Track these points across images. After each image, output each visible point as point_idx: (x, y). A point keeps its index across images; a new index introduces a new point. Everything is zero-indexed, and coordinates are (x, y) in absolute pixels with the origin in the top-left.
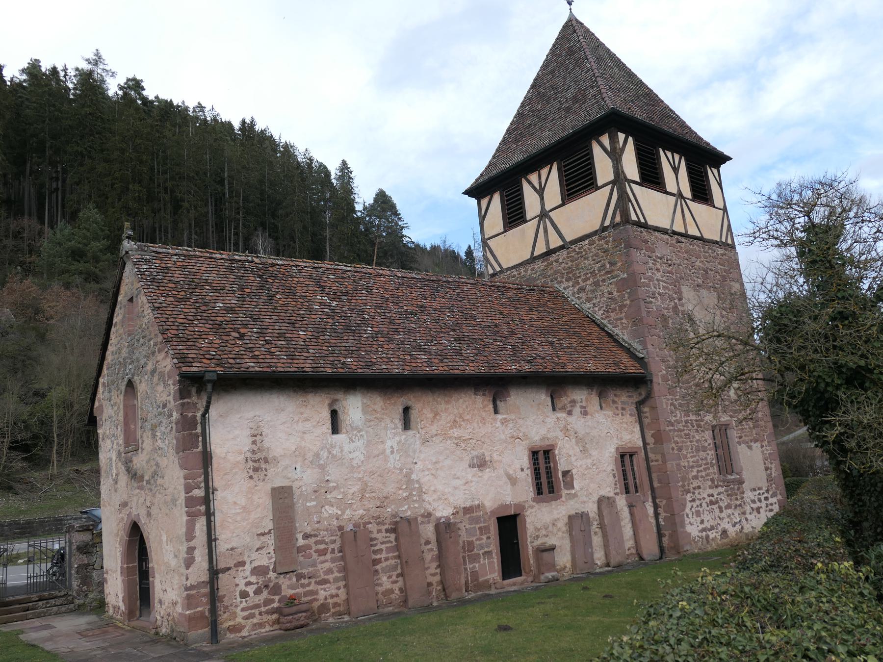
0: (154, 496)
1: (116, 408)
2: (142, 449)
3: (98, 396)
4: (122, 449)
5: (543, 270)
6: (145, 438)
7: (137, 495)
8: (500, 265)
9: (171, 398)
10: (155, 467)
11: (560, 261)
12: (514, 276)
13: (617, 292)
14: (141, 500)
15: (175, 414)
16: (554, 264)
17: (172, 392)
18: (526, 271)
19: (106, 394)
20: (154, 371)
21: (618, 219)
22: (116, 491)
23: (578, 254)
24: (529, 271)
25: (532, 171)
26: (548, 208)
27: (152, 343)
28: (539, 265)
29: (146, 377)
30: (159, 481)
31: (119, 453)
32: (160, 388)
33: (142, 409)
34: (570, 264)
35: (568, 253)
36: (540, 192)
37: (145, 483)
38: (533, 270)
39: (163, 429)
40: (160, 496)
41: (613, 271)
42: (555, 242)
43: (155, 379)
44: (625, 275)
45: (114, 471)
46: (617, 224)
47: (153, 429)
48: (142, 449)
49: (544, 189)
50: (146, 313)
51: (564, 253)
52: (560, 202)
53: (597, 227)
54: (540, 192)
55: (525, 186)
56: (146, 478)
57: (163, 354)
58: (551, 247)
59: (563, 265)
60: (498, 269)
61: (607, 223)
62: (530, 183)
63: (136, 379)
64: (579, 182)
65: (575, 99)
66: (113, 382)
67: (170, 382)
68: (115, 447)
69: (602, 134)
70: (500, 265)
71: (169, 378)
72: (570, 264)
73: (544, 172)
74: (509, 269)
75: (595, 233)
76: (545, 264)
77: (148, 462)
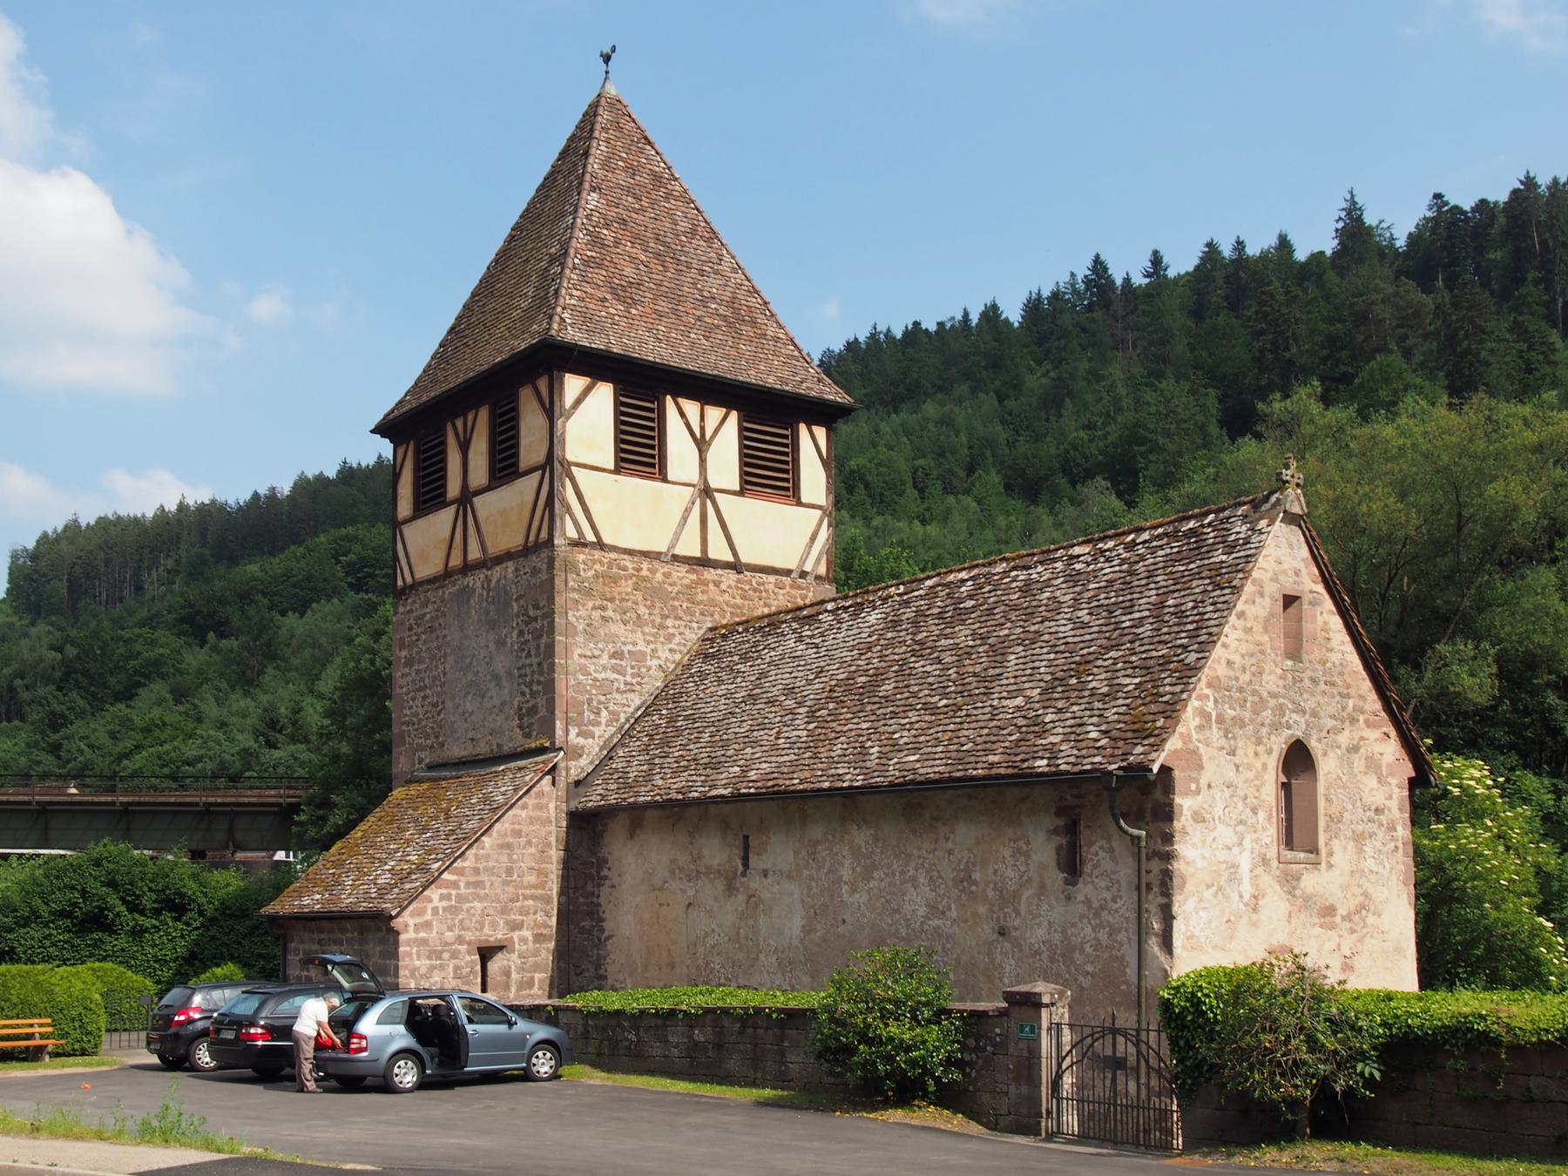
0: (1361, 940)
1: (1251, 775)
2: (1330, 866)
3: (1180, 729)
4: (1272, 853)
5: (690, 587)
6: (1336, 845)
7: (1319, 936)
9: (1394, 805)
10: (1361, 899)
11: (723, 586)
12: (625, 569)
15: (1399, 828)
16: (711, 586)
17: (1395, 796)
18: (653, 571)
19: (1215, 733)
20: (1354, 749)
21: (822, 570)
22: (1255, 924)
23: (755, 590)
24: (659, 576)
26: (713, 484)
28: (680, 573)
30: (1371, 920)
31: (1265, 861)
32: (1371, 781)
33: (1328, 800)
34: (739, 601)
35: (739, 581)
36: (702, 444)
37: (1338, 919)
38: (667, 575)
39: (1378, 844)
40: (1373, 941)
43: (1359, 763)
45: (1247, 888)
47: (1359, 839)
48: (1330, 866)
49: (704, 442)
51: (730, 577)
52: (737, 488)
56: (1342, 911)
58: (713, 554)
59: (726, 596)
60: (591, 537)
62: (682, 415)
64: (768, 473)
66: (1239, 722)
67: (1394, 781)
68: (1247, 842)
72: (739, 601)
73: (714, 414)
74: (614, 549)
75: (788, 572)
76: (694, 577)
77: (1344, 888)
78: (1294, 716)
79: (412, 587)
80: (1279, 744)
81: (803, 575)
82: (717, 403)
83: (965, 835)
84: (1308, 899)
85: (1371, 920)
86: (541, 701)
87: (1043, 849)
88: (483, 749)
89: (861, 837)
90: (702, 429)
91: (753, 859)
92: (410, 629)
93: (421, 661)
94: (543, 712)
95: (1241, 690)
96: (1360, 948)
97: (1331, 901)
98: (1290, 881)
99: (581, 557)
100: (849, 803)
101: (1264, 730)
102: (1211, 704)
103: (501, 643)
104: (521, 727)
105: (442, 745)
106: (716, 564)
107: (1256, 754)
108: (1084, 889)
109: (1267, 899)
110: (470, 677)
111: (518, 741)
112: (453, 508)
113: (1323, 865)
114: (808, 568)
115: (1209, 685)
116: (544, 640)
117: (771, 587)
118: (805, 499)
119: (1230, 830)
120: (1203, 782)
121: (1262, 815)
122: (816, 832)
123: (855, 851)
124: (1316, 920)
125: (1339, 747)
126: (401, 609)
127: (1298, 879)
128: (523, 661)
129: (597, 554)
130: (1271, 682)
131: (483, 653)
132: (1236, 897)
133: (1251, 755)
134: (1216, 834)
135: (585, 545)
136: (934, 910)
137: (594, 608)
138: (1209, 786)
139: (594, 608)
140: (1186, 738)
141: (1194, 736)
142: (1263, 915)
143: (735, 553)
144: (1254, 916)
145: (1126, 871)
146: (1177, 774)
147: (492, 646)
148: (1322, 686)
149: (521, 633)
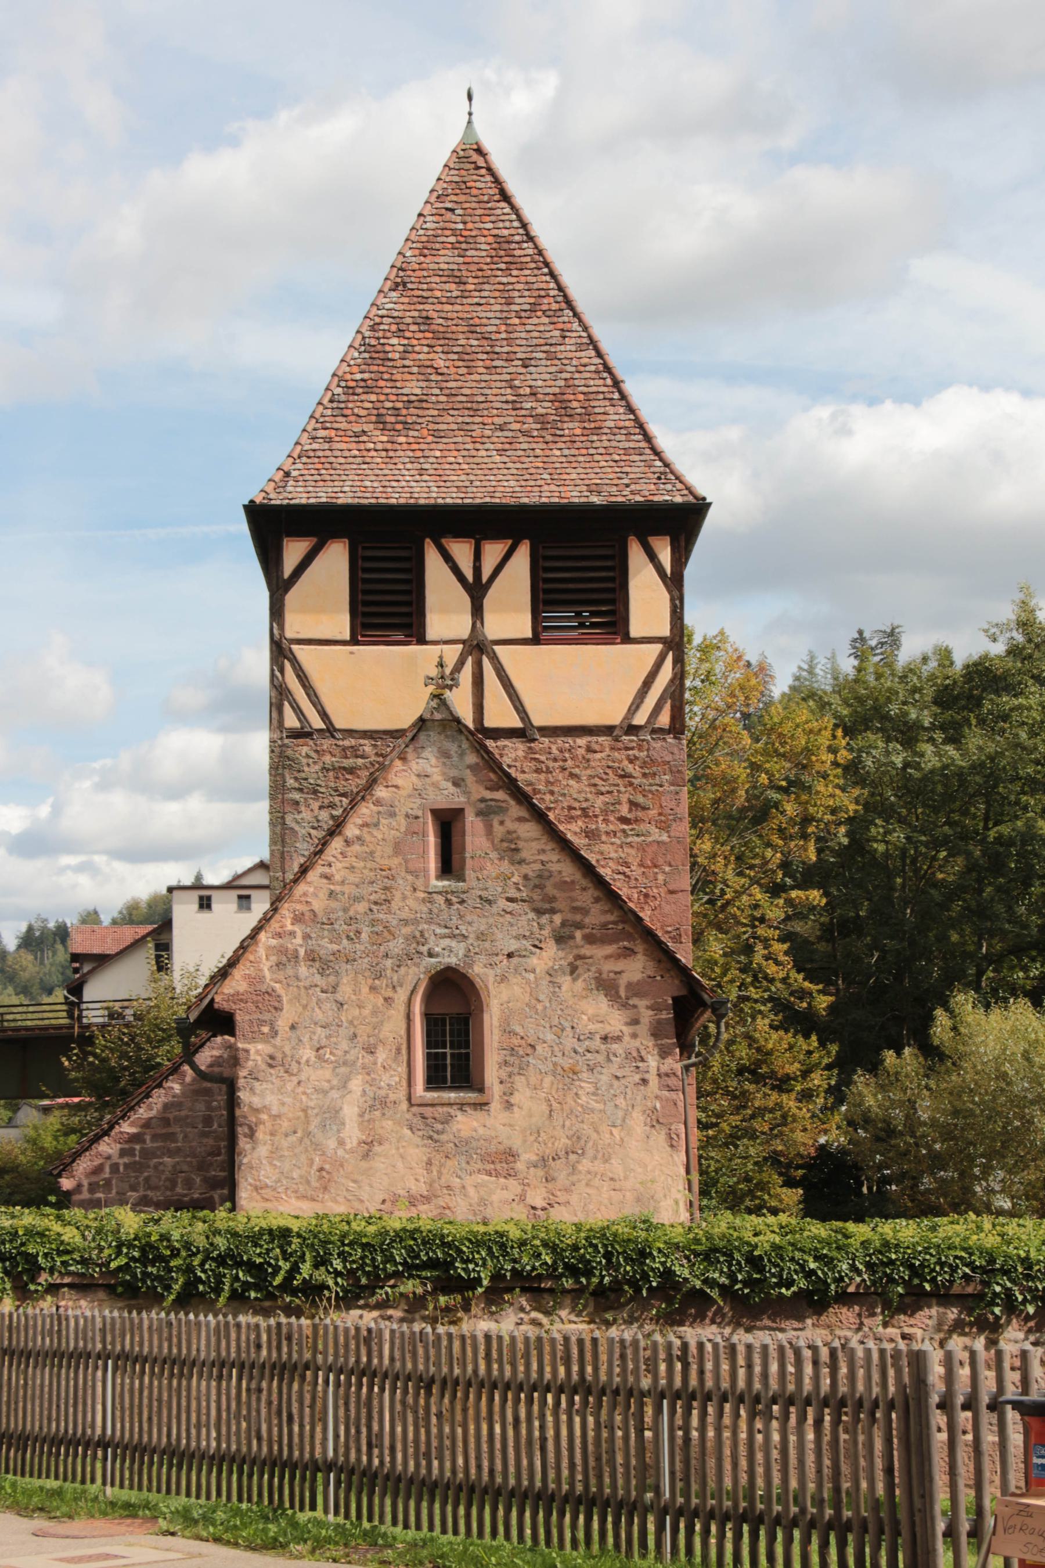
6: (519, 1081)
8: (324, 715)
13: (641, 865)
14: (508, 1195)
21: (664, 719)
23: (555, 760)
25: (460, 534)
27: (558, 919)
29: (531, 976)
36: (477, 591)
37: (520, 1166)
41: (637, 820)
42: (500, 714)
44: (665, 837)
45: (353, 1134)
46: (661, 730)
48: (509, 1106)
50: (524, 854)
52: (529, 634)
53: (615, 717)
54: (477, 591)
55: (433, 559)
56: (528, 1156)
57: (610, 949)
58: (489, 722)
60: (318, 723)
61: (640, 719)
62: (448, 558)
63: (479, 971)
65: (560, 401)
68: (356, 1084)
69: (658, 532)
70: (324, 715)
71: (637, 995)
74: (350, 733)
78: (447, 942)
80: (417, 974)
81: (632, 729)
82: (496, 535)
84: (463, 1146)
85: (585, 1165)
90: (477, 570)
95: (351, 920)
96: (562, 1197)
97: (507, 1143)
98: (429, 1125)
99: (305, 750)
101: (389, 963)
102: (299, 940)
106: (497, 733)
107: (373, 989)
109: (387, 1146)
113: (495, 1106)
114: (640, 719)
115: (298, 919)
117: (582, 751)
118: (634, 632)
119: (327, 1074)
120: (282, 1024)
121: (382, 1055)
124: (479, 1165)
125: (534, 971)
127: (447, 1120)
129: (326, 743)
130: (407, 903)
132: (332, 1143)
133: (365, 990)
134: (303, 1077)
135: (309, 735)
137: (321, 808)
138: (293, 1027)
139: (321, 808)
140: (256, 980)
141: (267, 974)
142: (379, 1164)
143: (522, 719)
144: (364, 1164)
146: (238, 1018)
148: (502, 903)
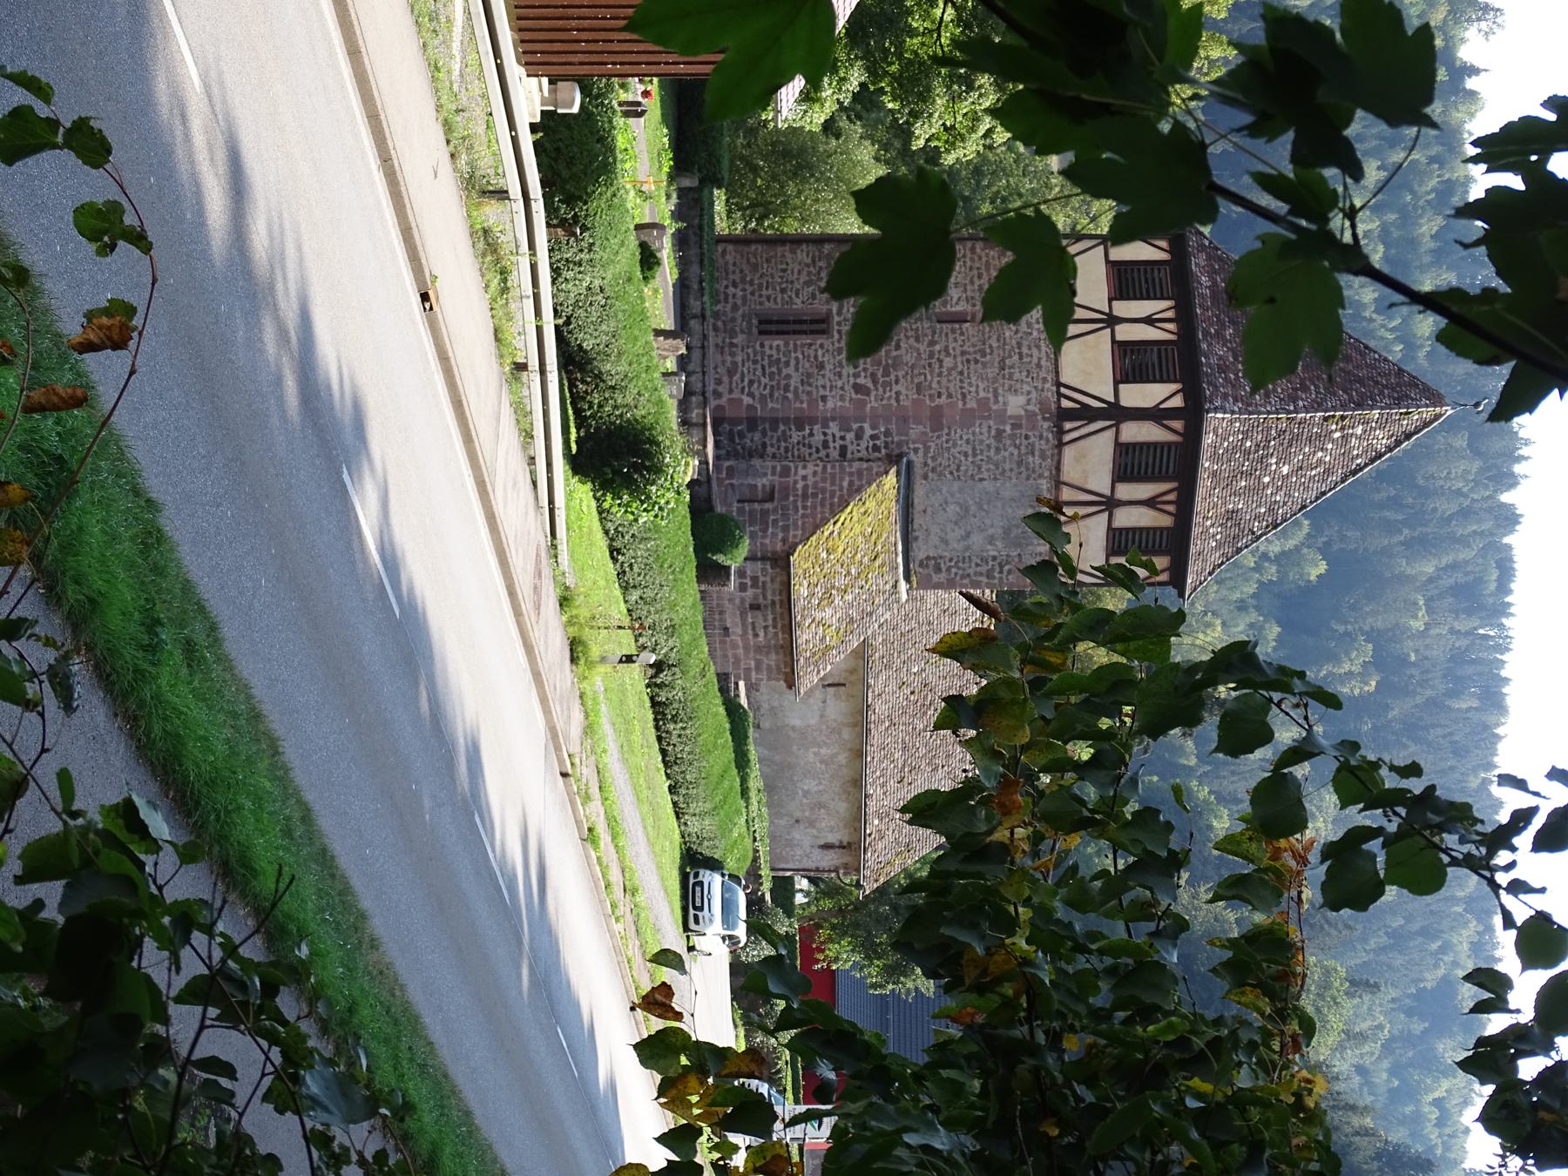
79: (1060, 440)
83: (842, 807)
86: (943, 577)
87: (832, 838)
88: (918, 520)
89: (843, 758)
91: (831, 690)
92: (1027, 437)
93: (998, 450)
94: (935, 578)
100: (859, 754)
103: (991, 540)
104: (928, 558)
105: (925, 477)
108: (817, 851)
110: (973, 508)
111: (920, 552)
112: (1107, 492)
116: (984, 580)
122: (847, 734)
123: (835, 755)
126: (1046, 425)
128: (975, 560)
131: (988, 522)
136: (806, 793)
145: (824, 864)
147: (991, 531)
149: (994, 558)
